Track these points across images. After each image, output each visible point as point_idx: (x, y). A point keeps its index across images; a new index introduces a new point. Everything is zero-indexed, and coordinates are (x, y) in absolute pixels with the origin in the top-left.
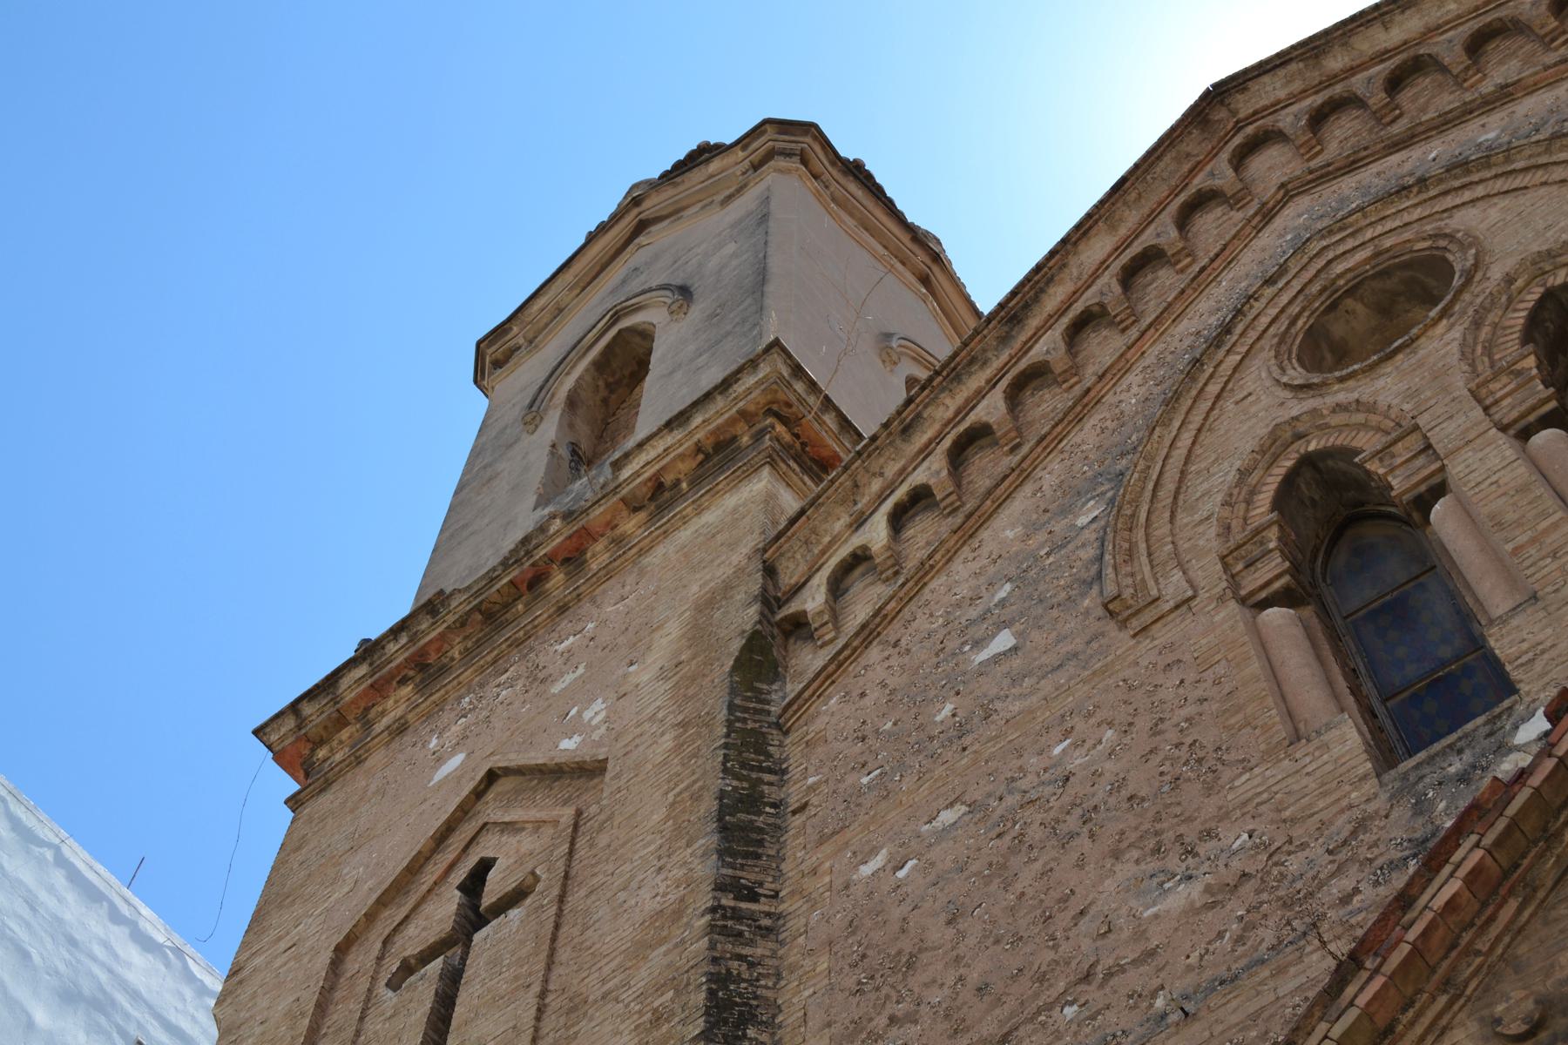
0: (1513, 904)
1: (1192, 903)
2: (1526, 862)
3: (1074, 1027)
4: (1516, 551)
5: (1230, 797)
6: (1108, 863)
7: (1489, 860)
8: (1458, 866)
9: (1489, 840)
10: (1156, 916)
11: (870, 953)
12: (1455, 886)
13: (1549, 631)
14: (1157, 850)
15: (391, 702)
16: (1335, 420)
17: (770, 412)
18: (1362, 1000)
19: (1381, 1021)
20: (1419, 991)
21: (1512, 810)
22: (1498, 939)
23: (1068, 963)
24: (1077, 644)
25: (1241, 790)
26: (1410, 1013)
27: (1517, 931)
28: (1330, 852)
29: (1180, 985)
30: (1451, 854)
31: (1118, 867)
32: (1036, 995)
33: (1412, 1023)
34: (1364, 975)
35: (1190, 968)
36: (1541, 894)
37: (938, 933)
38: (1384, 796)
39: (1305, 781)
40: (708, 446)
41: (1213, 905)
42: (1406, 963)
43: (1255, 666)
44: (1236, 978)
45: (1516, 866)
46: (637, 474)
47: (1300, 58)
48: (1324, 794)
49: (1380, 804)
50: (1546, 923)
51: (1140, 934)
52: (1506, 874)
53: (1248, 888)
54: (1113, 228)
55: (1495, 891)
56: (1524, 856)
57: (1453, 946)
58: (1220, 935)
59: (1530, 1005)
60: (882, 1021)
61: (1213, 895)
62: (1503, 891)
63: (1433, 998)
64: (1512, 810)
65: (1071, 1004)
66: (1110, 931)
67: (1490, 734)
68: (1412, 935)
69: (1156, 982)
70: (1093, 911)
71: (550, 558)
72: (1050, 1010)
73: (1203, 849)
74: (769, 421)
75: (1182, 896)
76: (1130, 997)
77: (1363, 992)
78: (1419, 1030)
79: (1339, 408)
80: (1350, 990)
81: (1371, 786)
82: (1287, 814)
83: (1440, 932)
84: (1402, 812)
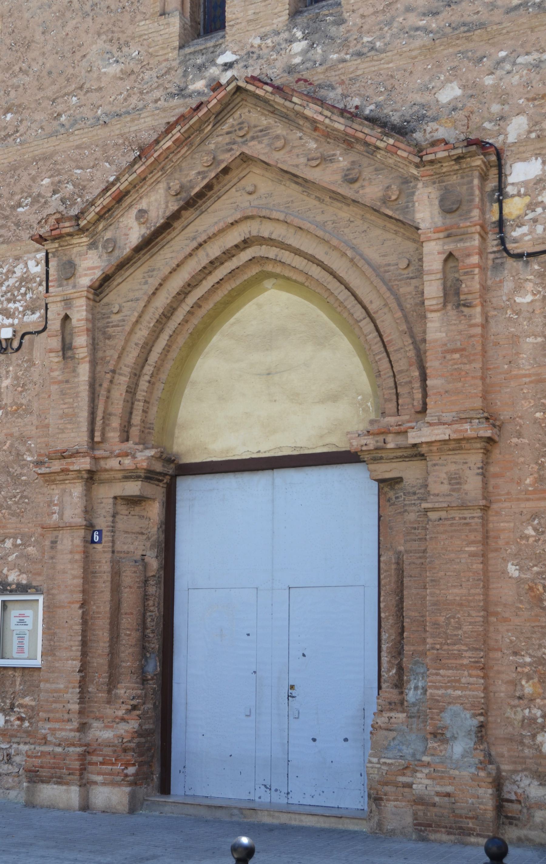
0: (185, 149)
1: (116, 74)
2: (192, 137)
3: (74, 108)
5: (137, 30)
6: (96, 36)
7: (182, 136)
8: (173, 136)
9: (182, 131)
10: (105, 73)
11: (16, 30)
12: (169, 143)
13: (242, 14)
14: (111, 41)
18: (138, 172)
19: (143, 177)
20: (155, 169)
21: (191, 122)
22: (179, 159)
23: (77, 78)
25: (141, 28)
26: (151, 175)
27: (184, 157)
28: (157, 77)
29: (107, 108)
30: (173, 130)
31: (98, 41)
32: (65, 87)
33: (151, 178)
34: (141, 163)
35: (110, 103)
36: (194, 148)
37: (38, 37)
38: (178, 61)
39: (160, 38)
41: (121, 79)
42: (152, 164)
44: (121, 115)
45: (189, 137)
48: (163, 48)
49: (175, 64)
50: (192, 158)
51: (99, 79)
52: (186, 139)
53: (133, 77)
55: (182, 144)
56: (192, 134)
57: (167, 158)
58: (121, 94)
59: (178, 187)
61: (123, 74)
62: (184, 144)
63: (158, 172)
64: (191, 122)
65: (76, 96)
66: (91, 70)
67: (213, 52)
68: (156, 155)
69: (100, 103)
70: (88, 57)
72: (69, 95)
73: (125, 49)
76: (92, 104)
77: (140, 168)
78: (152, 180)
80: (136, 166)
82: (151, 50)
83: (164, 154)
84: (180, 71)
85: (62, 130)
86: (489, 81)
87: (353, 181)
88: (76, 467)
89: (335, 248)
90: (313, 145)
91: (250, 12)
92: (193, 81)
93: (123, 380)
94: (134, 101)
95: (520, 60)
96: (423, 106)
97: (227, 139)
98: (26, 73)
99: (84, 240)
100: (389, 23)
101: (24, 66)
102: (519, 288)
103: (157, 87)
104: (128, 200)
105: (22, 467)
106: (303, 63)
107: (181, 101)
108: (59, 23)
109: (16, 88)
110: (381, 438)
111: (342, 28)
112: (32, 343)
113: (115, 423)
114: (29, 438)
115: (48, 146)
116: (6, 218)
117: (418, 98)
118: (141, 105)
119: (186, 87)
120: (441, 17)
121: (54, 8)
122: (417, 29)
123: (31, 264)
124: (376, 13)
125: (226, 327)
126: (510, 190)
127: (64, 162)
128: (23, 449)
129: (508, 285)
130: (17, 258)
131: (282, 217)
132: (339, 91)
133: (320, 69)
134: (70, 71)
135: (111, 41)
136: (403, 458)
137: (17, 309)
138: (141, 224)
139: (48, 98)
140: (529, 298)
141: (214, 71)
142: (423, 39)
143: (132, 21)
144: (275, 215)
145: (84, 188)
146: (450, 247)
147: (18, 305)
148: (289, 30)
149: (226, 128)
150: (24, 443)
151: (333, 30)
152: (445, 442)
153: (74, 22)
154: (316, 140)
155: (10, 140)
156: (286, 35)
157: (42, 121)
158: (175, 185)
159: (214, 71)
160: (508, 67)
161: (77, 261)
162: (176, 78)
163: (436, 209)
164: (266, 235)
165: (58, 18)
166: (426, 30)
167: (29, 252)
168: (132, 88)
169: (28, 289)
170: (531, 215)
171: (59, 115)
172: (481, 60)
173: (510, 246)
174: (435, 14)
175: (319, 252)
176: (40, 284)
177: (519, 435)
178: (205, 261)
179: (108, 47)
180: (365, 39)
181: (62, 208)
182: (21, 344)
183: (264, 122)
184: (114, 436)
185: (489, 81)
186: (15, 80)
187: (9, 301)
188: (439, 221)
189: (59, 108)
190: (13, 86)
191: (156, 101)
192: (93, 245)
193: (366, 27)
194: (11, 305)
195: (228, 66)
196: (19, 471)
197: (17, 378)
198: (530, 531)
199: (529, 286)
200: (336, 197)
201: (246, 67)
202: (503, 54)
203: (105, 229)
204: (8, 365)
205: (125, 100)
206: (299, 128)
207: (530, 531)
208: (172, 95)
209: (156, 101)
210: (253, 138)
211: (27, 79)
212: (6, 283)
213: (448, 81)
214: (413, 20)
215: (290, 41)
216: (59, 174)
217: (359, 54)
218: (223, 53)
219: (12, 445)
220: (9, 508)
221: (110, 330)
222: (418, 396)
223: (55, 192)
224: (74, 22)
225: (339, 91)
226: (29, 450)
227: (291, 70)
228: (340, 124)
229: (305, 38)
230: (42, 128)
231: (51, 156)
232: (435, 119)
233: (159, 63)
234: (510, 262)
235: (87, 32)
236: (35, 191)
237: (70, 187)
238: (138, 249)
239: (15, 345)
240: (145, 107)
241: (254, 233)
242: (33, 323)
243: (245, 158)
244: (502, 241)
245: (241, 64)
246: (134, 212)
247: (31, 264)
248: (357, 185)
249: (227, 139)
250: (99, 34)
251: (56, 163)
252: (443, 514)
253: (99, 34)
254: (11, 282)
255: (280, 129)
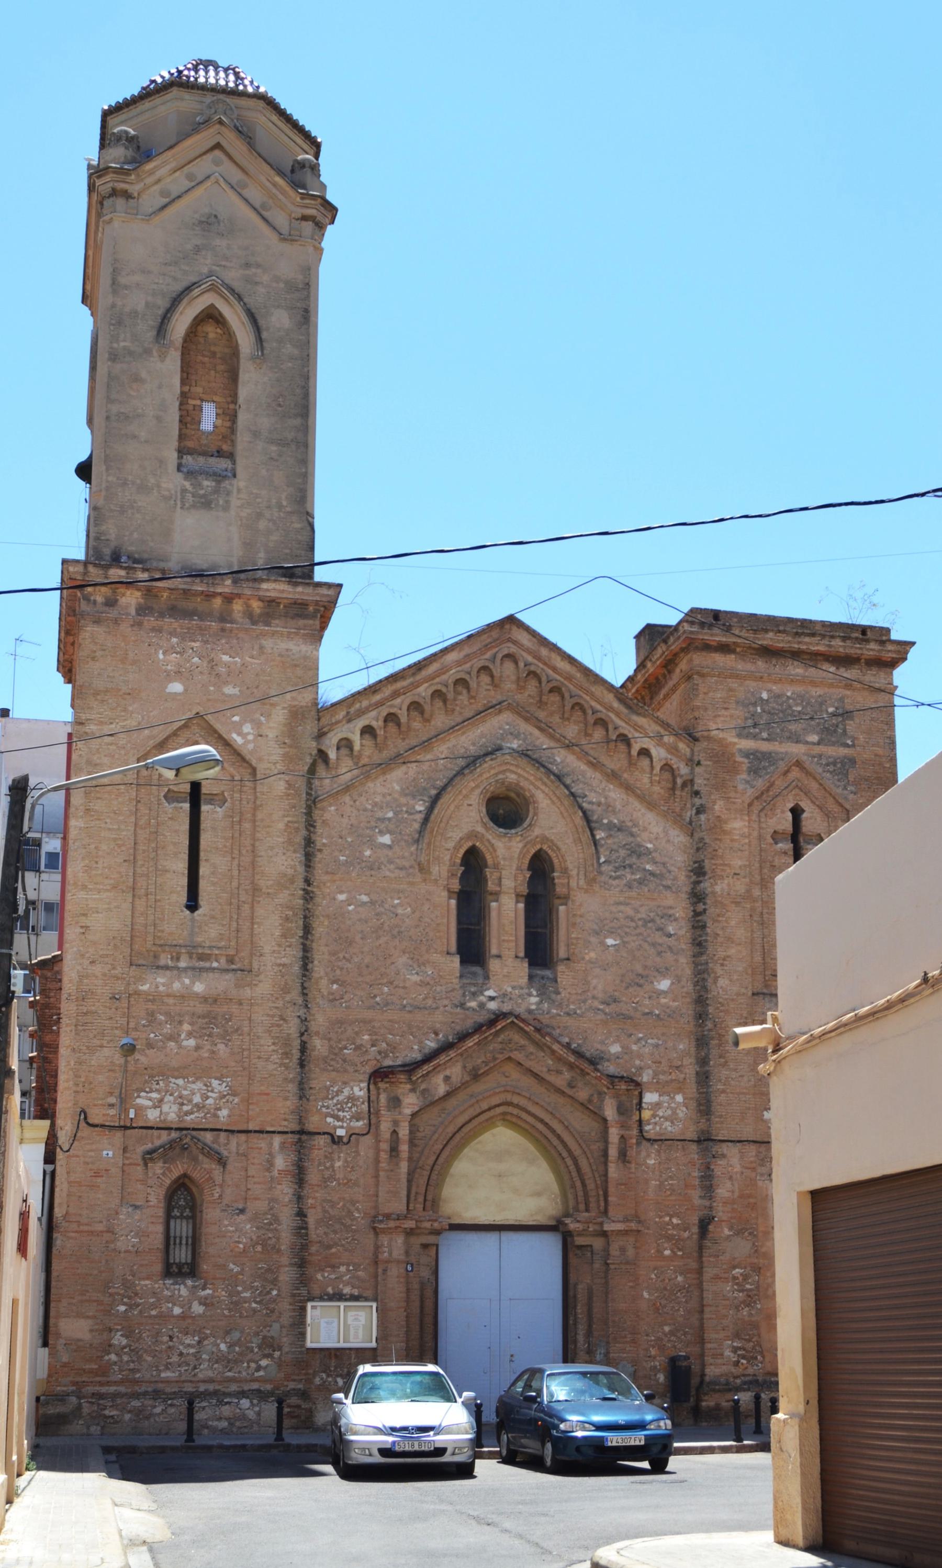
4: (504, 941)
15: (128, 592)
16: (487, 844)
17: (324, 607)
24: (407, 864)
40: (300, 601)
43: (445, 921)
46: (268, 590)
47: (538, 640)
49: (457, 987)
51: (404, 981)
54: (460, 651)
60: (341, 955)
71: (220, 594)
73: (423, 968)
74: (322, 609)
75: (415, 978)
79: (488, 840)
81: (457, 981)
84: (461, 992)
85: (378, 1007)
86: (634, 1047)
87: (573, 1087)
88: (406, 1226)
89: (556, 1118)
90: (550, 1062)
91: (505, 971)
92: (469, 1001)
93: (426, 1173)
94: (430, 1002)
95: (649, 1041)
96: (602, 1052)
97: (500, 1046)
98: (349, 961)
99: (408, 1086)
100: (584, 1001)
101: (346, 955)
102: (648, 1156)
103: (446, 998)
104: (439, 1069)
105: (352, 1220)
106: (537, 1009)
107: (462, 1011)
108: (374, 935)
109: (342, 969)
110: (586, 1225)
111: (559, 997)
112: (358, 1141)
113: (421, 1199)
114: (358, 1202)
115: (368, 1014)
116: (336, 1054)
117: (599, 1047)
118: (434, 1006)
119: (465, 1004)
120: (611, 1007)
121: (370, 924)
122: (599, 1010)
123: (356, 1089)
124: (576, 994)
125: (472, 1144)
126: (643, 1105)
127: (380, 1028)
128: (352, 1209)
129: (643, 1154)
130: (345, 1083)
131: (528, 1095)
132: (558, 1031)
133: (547, 1016)
134: (383, 970)
135: (412, 959)
136: (594, 1235)
137: (345, 1116)
138: (445, 1084)
139: (367, 983)
140: (652, 1162)
141: (482, 998)
142: (600, 1016)
143: (427, 951)
144: (524, 1093)
145: (395, 1048)
146: (622, 1132)
147: (345, 1114)
148: (529, 989)
149: (500, 1039)
150: (354, 1205)
151: (553, 996)
152: (620, 1231)
153: (385, 939)
154: (552, 1060)
155: (337, 1003)
156: (527, 991)
157: (361, 997)
158: (469, 1066)
159: (482, 998)
160: (643, 1043)
161: (401, 1097)
162: (457, 996)
163: (615, 1111)
164: (516, 1102)
165: (373, 932)
166: (602, 1011)
167: (354, 1081)
168: (428, 993)
169: (354, 1105)
170: (653, 1121)
171: (375, 996)
172: (631, 1035)
173: (645, 1134)
174: (608, 1004)
175: (547, 1119)
176: (363, 1103)
177: (648, 1229)
178: (478, 1111)
179: (410, 962)
180: (572, 1007)
181: (379, 1057)
182: (349, 1140)
183: (523, 1042)
184: (420, 1207)
185: (634, 1047)
186: (340, 963)
187: (339, 1110)
188: (616, 1117)
189: (376, 992)
190: (338, 967)
191: (445, 1006)
192: (413, 1090)
193: (571, 1000)
194: (340, 1113)
195: (492, 999)
196: (350, 1222)
197: (346, 1161)
198: (653, 1276)
199: (653, 1155)
200: (563, 1093)
201: (503, 1002)
202: (641, 1035)
203: (422, 1082)
204: (340, 1152)
205: (424, 999)
206: (543, 1051)
207: (653, 1276)
208: (457, 1006)
209: (445, 1006)
210: (516, 1050)
211: (349, 965)
212: (336, 1098)
213: (614, 1042)
214: (596, 1004)
215: (530, 995)
216: (376, 1035)
217: (568, 1014)
218: (488, 989)
219: (344, 1205)
220: (343, 1245)
221: (416, 1142)
222: (602, 1204)
223: (373, 1045)
224: (385, 939)
225: (558, 1031)
226: (357, 1209)
227: (530, 1012)
228: (572, 1058)
229: (538, 996)
230: (362, 1001)
231: (370, 1021)
232: (608, 1060)
233: (447, 983)
234: (644, 1142)
235: (395, 948)
236: (358, 1042)
237: (384, 1045)
238: (440, 1099)
239: (345, 1140)
240: (437, 1008)
241: (509, 1100)
242: (358, 1128)
243: (509, 1058)
244: (641, 1131)
245: (500, 1000)
246: (441, 1076)
247: (356, 1089)
248: (574, 1090)
249: (500, 1046)
250: (404, 952)
251: (374, 1027)
252: (617, 1266)
253: (404, 952)
254: (341, 1098)
255: (531, 1049)
